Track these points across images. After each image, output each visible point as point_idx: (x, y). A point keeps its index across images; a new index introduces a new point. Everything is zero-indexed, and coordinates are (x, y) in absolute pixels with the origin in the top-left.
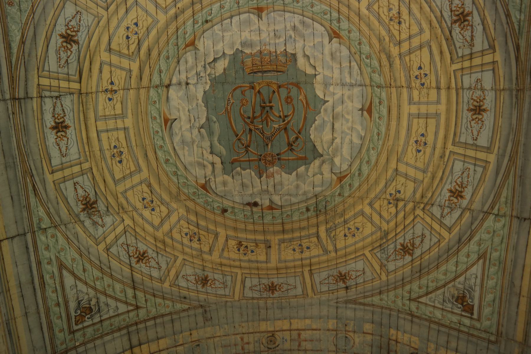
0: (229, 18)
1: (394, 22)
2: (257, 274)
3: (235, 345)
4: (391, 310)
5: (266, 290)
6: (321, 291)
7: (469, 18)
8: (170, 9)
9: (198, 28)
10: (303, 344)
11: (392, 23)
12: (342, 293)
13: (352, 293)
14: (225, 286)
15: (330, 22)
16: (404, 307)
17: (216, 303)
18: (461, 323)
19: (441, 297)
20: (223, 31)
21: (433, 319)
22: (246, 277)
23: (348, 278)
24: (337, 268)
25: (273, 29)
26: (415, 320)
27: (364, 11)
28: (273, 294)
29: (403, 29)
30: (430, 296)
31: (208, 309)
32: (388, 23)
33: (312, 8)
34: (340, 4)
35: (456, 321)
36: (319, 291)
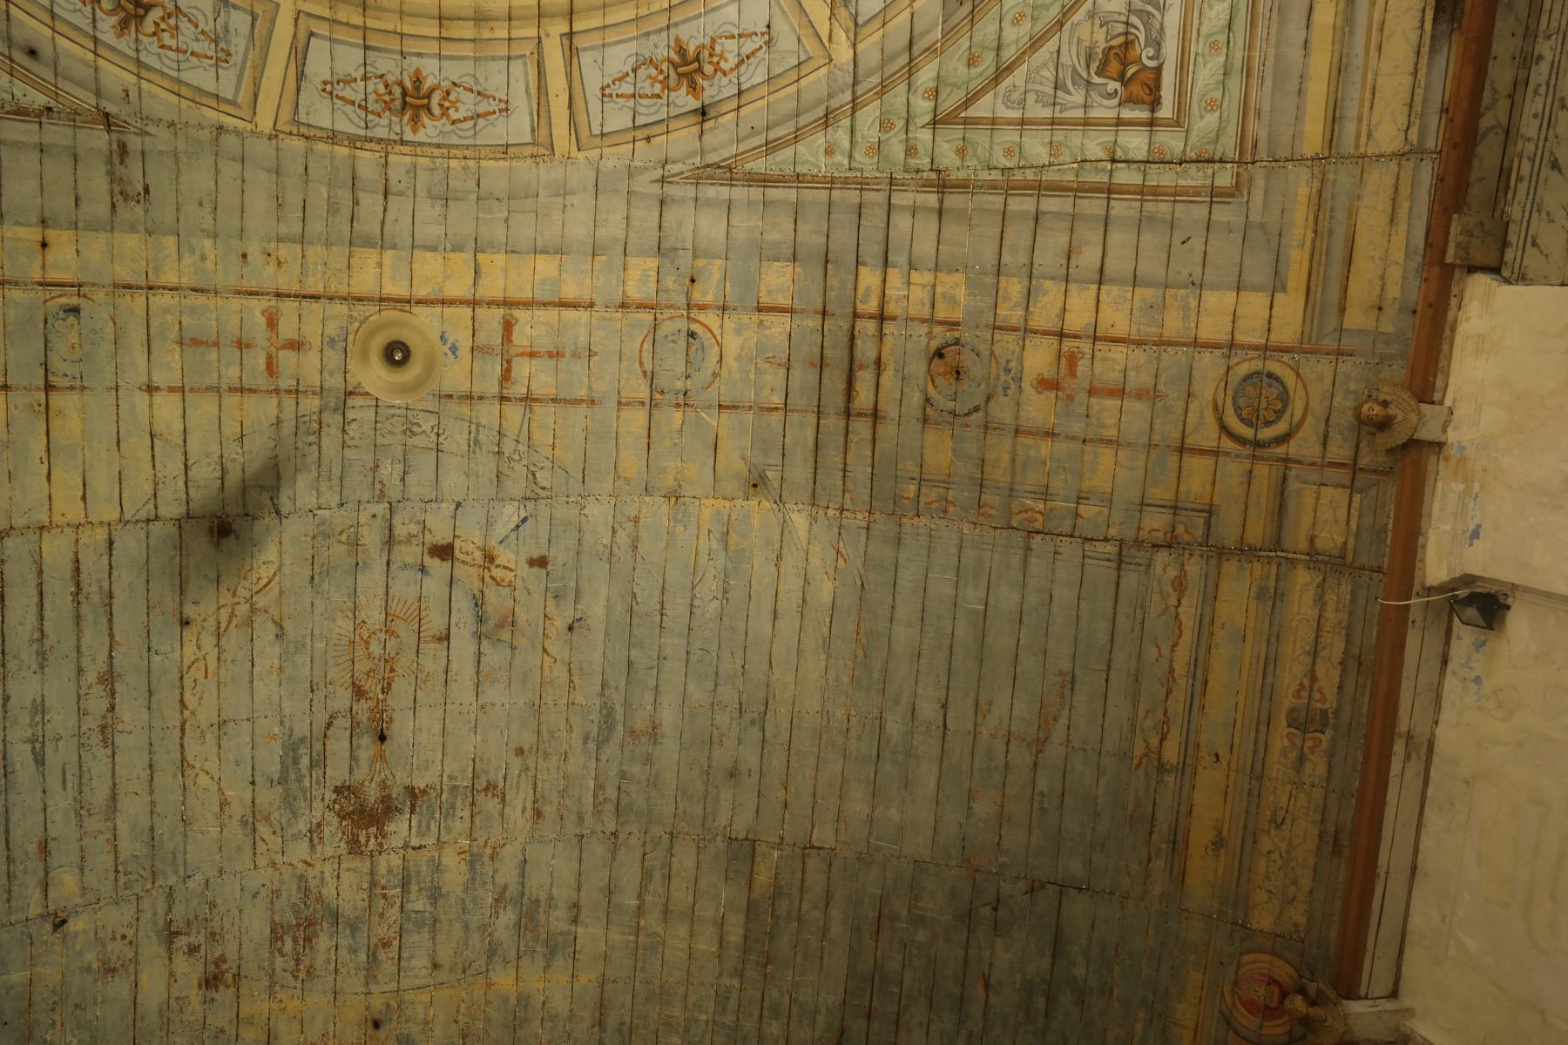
2: (356, 27)
3: (242, 345)
4: (863, 184)
5: (388, 106)
6: (605, 131)
10: (522, 368)
12: (683, 138)
13: (722, 140)
14: (221, 55)
16: (912, 162)
17: (172, 124)
18: (1119, 154)
19: (1048, 74)
21: (1018, 176)
22: (312, 34)
23: (708, 69)
24: (668, 27)
26: (954, 201)
28: (415, 131)
30: (1007, 82)
31: (134, 143)
35: (1101, 155)
36: (596, 131)
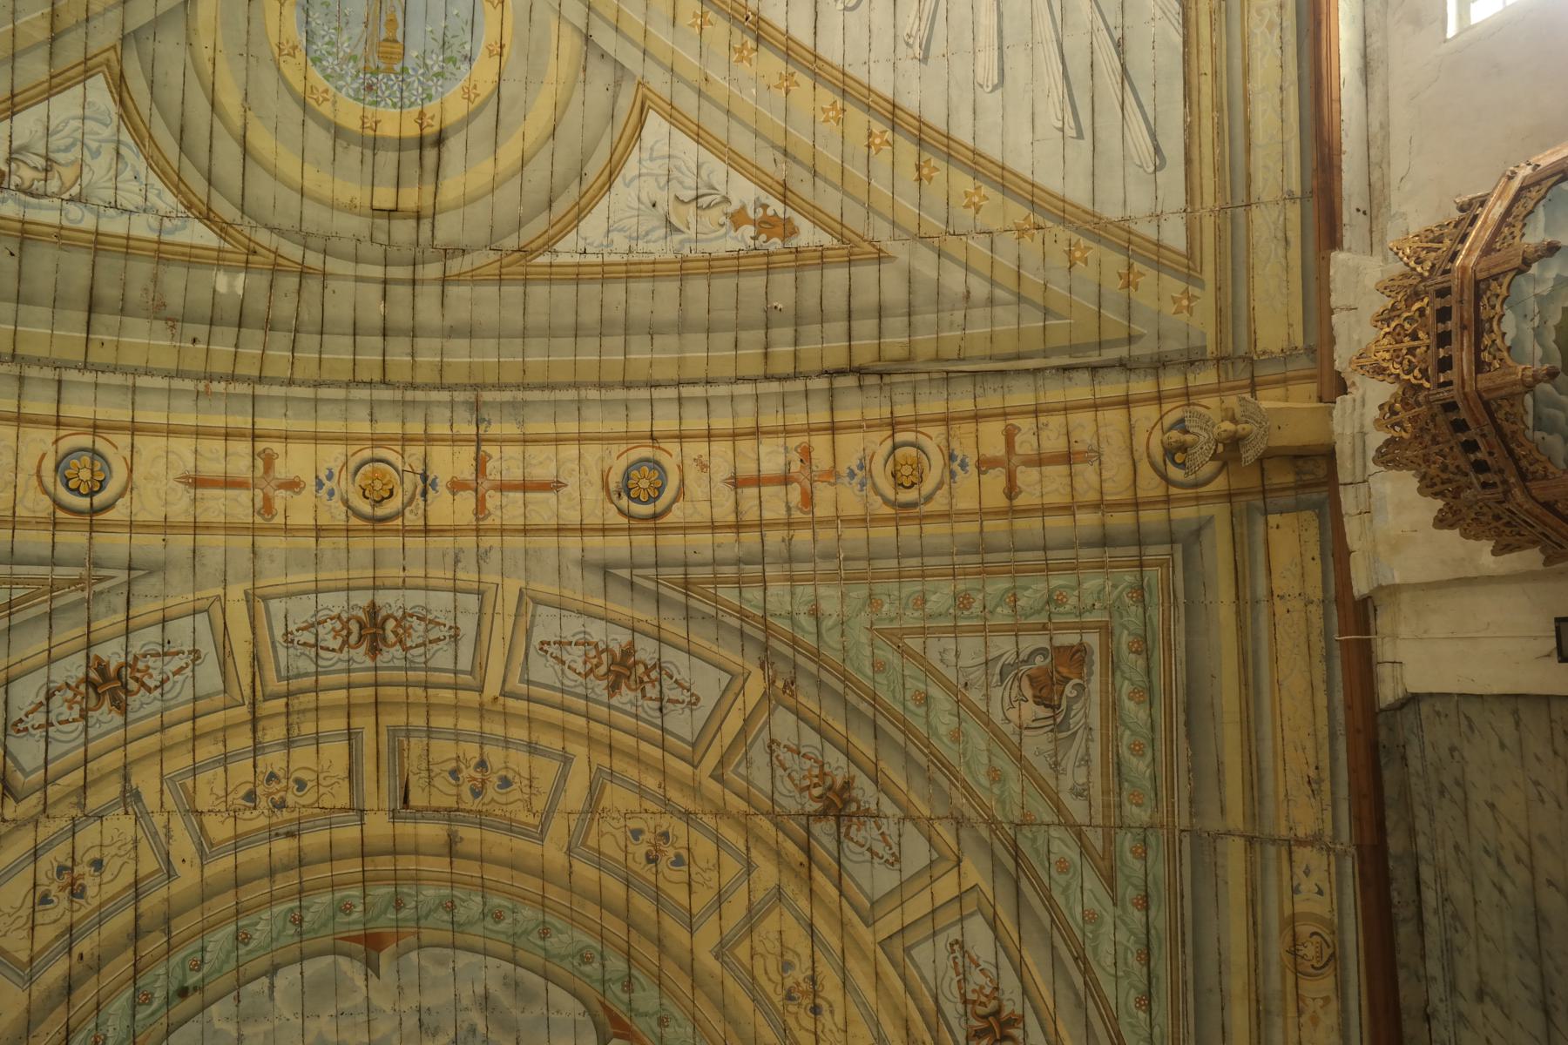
0: (264, 974)
1: (799, 1005)
7: (1016, 1032)
8: (48, 963)
9: (152, 1020)
11: (792, 1008)
15: (600, 989)
20: (241, 1020)
25: (414, 1005)
27: (707, 961)
29: (826, 1030)
32: (779, 1006)
33: (544, 939)
34: (633, 932)
